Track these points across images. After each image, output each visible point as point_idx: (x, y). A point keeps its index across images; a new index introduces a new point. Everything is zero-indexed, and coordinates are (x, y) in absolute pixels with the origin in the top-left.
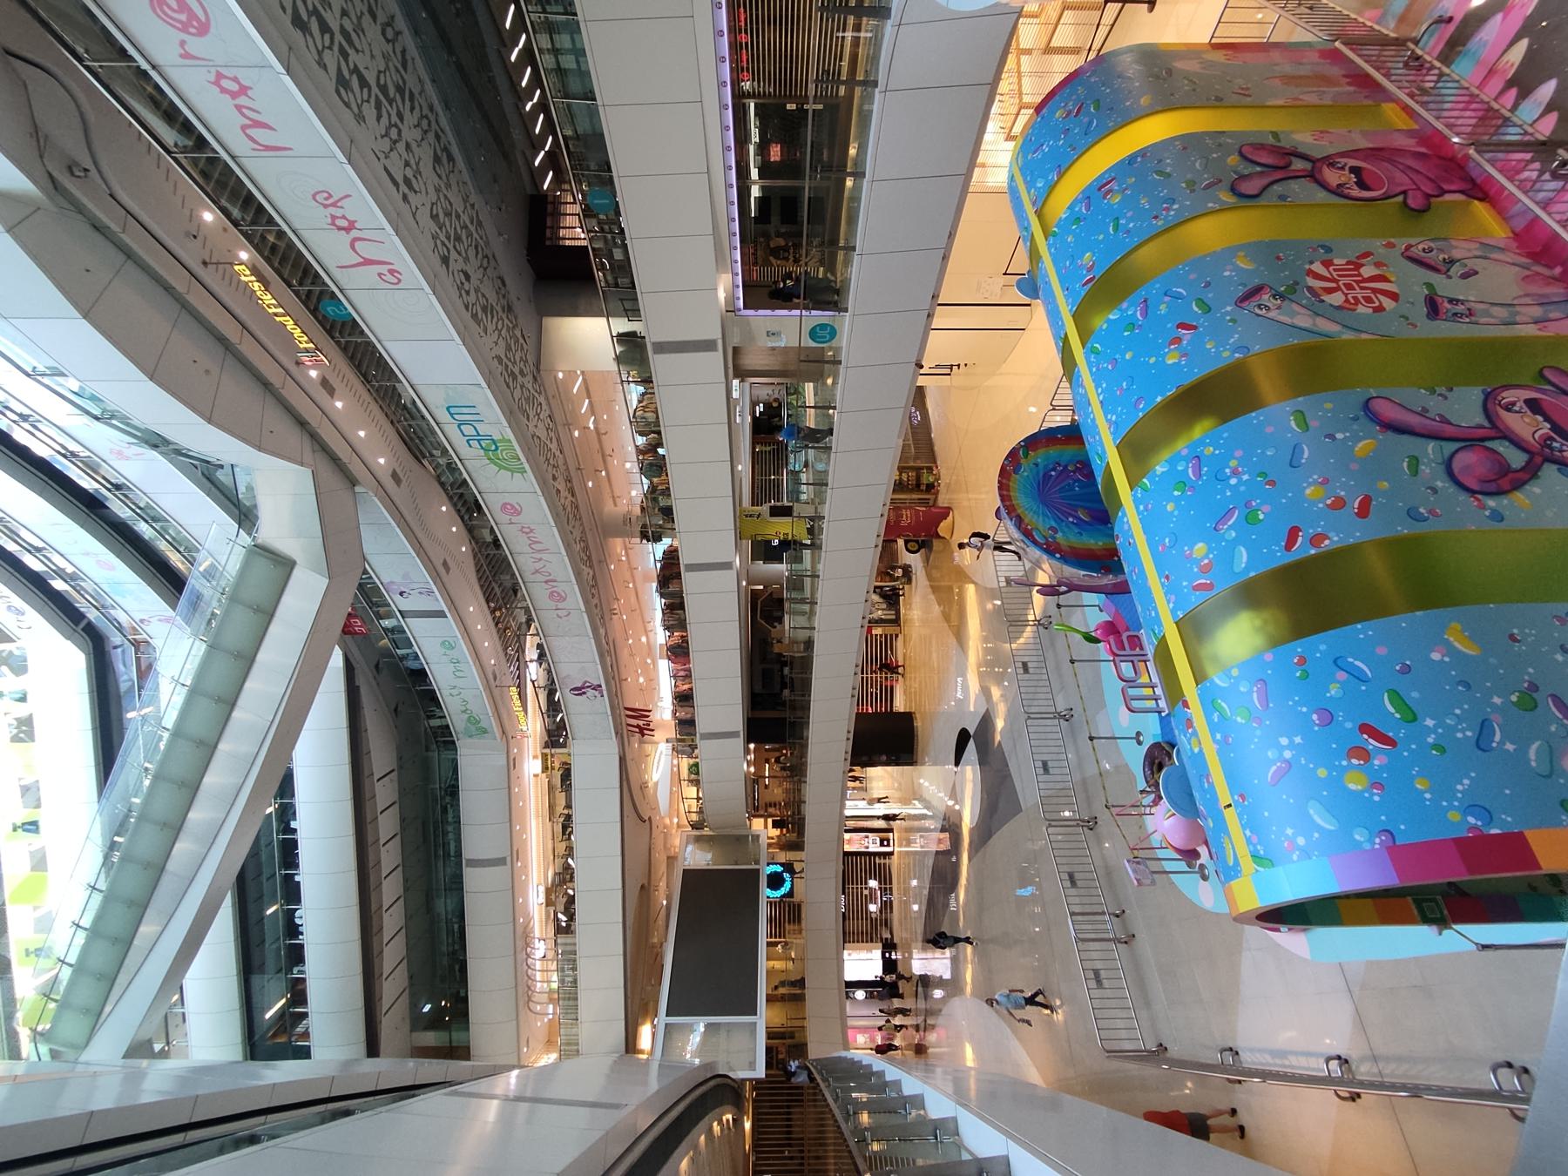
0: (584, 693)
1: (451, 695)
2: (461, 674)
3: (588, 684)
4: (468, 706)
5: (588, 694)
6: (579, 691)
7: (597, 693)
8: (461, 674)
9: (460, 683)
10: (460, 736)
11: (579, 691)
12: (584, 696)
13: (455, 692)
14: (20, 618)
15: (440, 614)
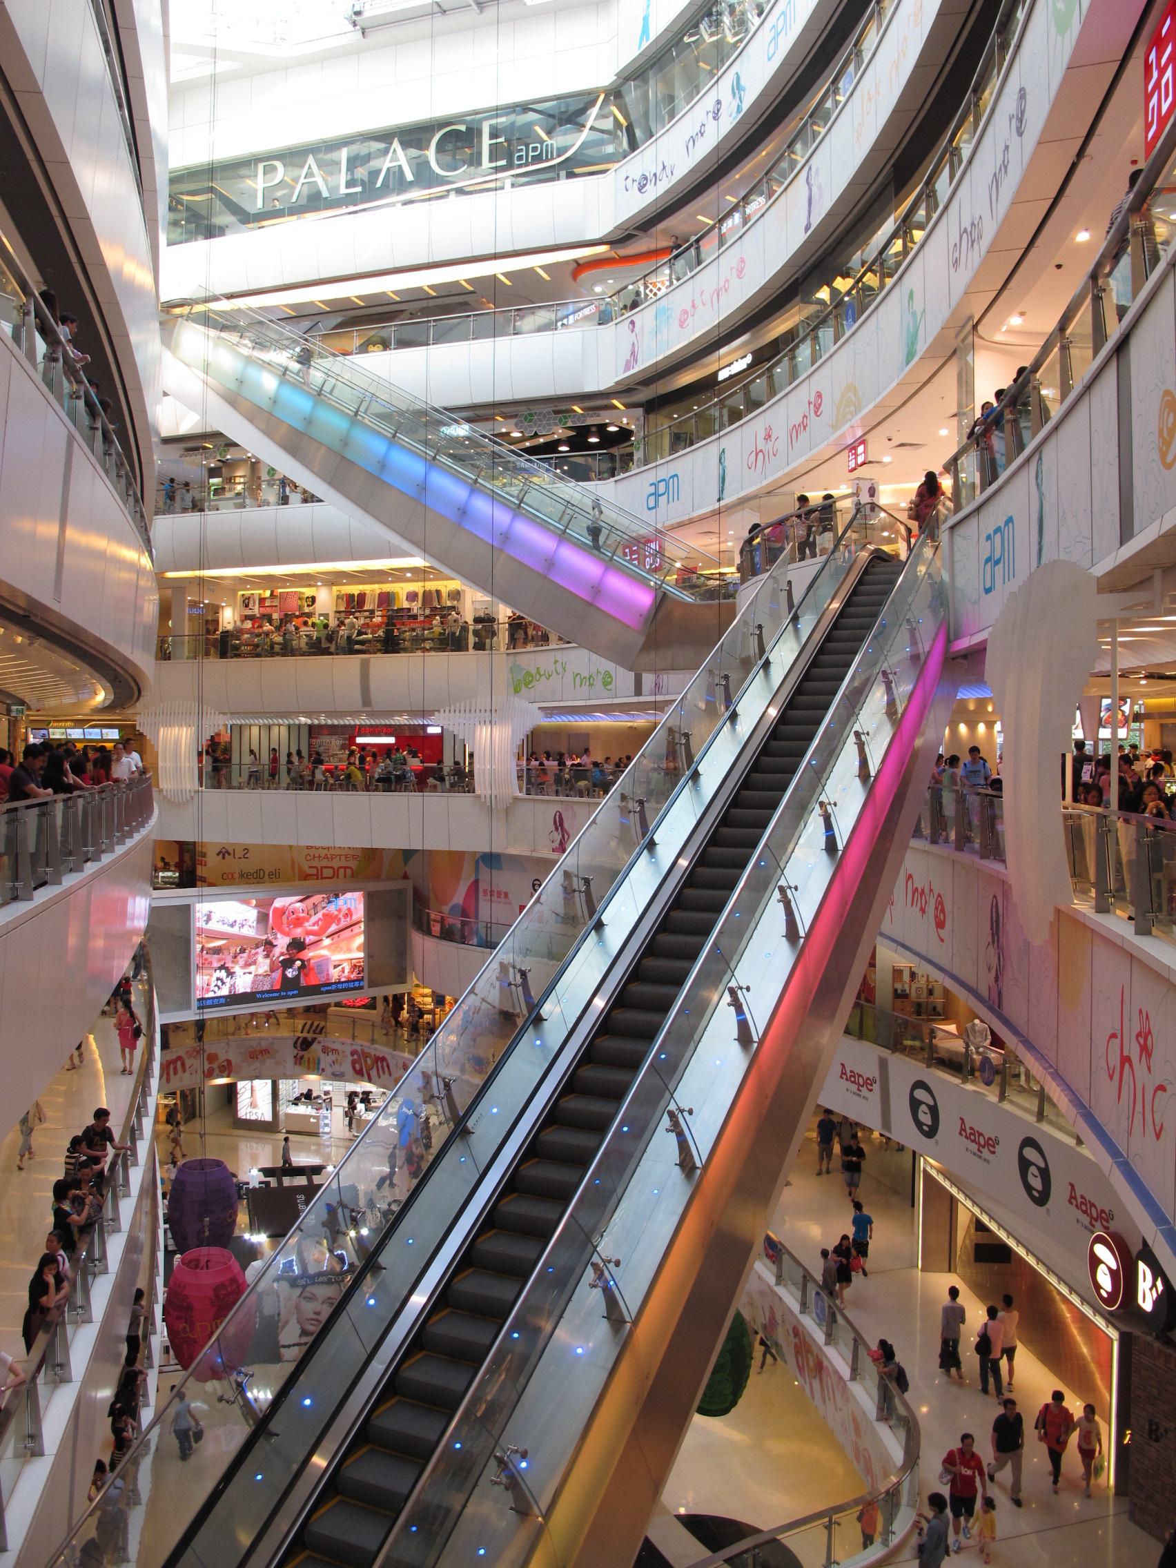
0: (557, 829)
1: (556, 662)
2: (578, 678)
3: (566, 836)
4: (543, 677)
5: (555, 833)
6: (559, 823)
7: (557, 844)
8: (578, 678)
9: (568, 677)
10: (511, 658)
11: (559, 823)
12: (553, 828)
13: (560, 669)
14: (636, 184)
15: (638, 692)
